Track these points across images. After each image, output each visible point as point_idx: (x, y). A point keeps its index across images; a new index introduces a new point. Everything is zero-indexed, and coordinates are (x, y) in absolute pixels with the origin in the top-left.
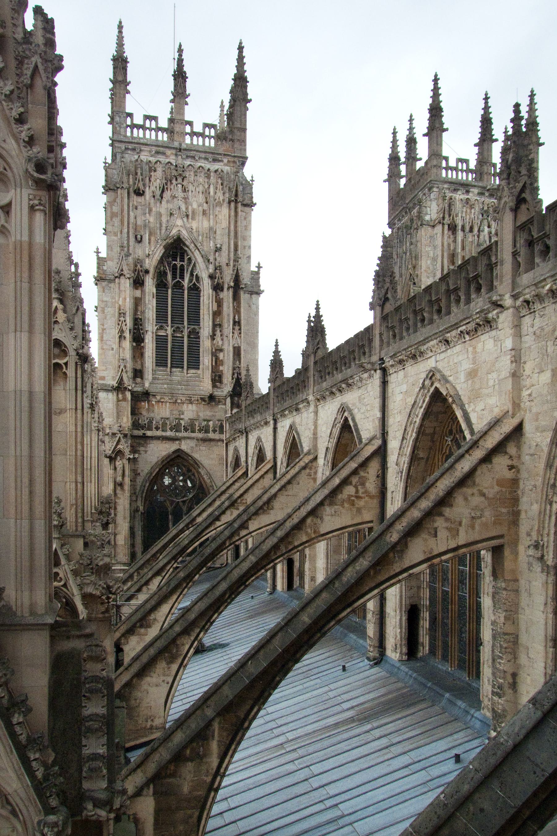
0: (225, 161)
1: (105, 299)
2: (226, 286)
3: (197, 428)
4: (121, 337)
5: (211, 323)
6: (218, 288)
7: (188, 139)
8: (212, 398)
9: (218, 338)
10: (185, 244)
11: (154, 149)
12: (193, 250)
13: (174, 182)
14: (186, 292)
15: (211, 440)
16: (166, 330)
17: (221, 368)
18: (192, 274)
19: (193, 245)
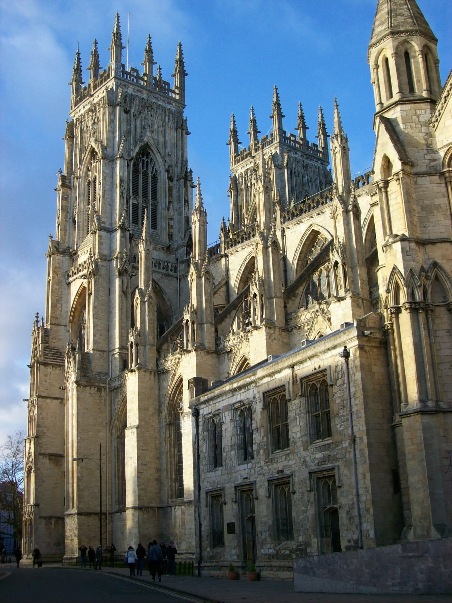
0: (174, 104)
1: (107, 172)
2: (175, 179)
3: (162, 266)
4: (121, 196)
5: (167, 200)
6: (171, 179)
8: (168, 248)
9: (171, 211)
10: (150, 149)
11: (136, 88)
12: (155, 153)
13: (146, 109)
15: (170, 276)
16: (138, 200)
17: (172, 230)
18: (153, 169)
19: (156, 150)
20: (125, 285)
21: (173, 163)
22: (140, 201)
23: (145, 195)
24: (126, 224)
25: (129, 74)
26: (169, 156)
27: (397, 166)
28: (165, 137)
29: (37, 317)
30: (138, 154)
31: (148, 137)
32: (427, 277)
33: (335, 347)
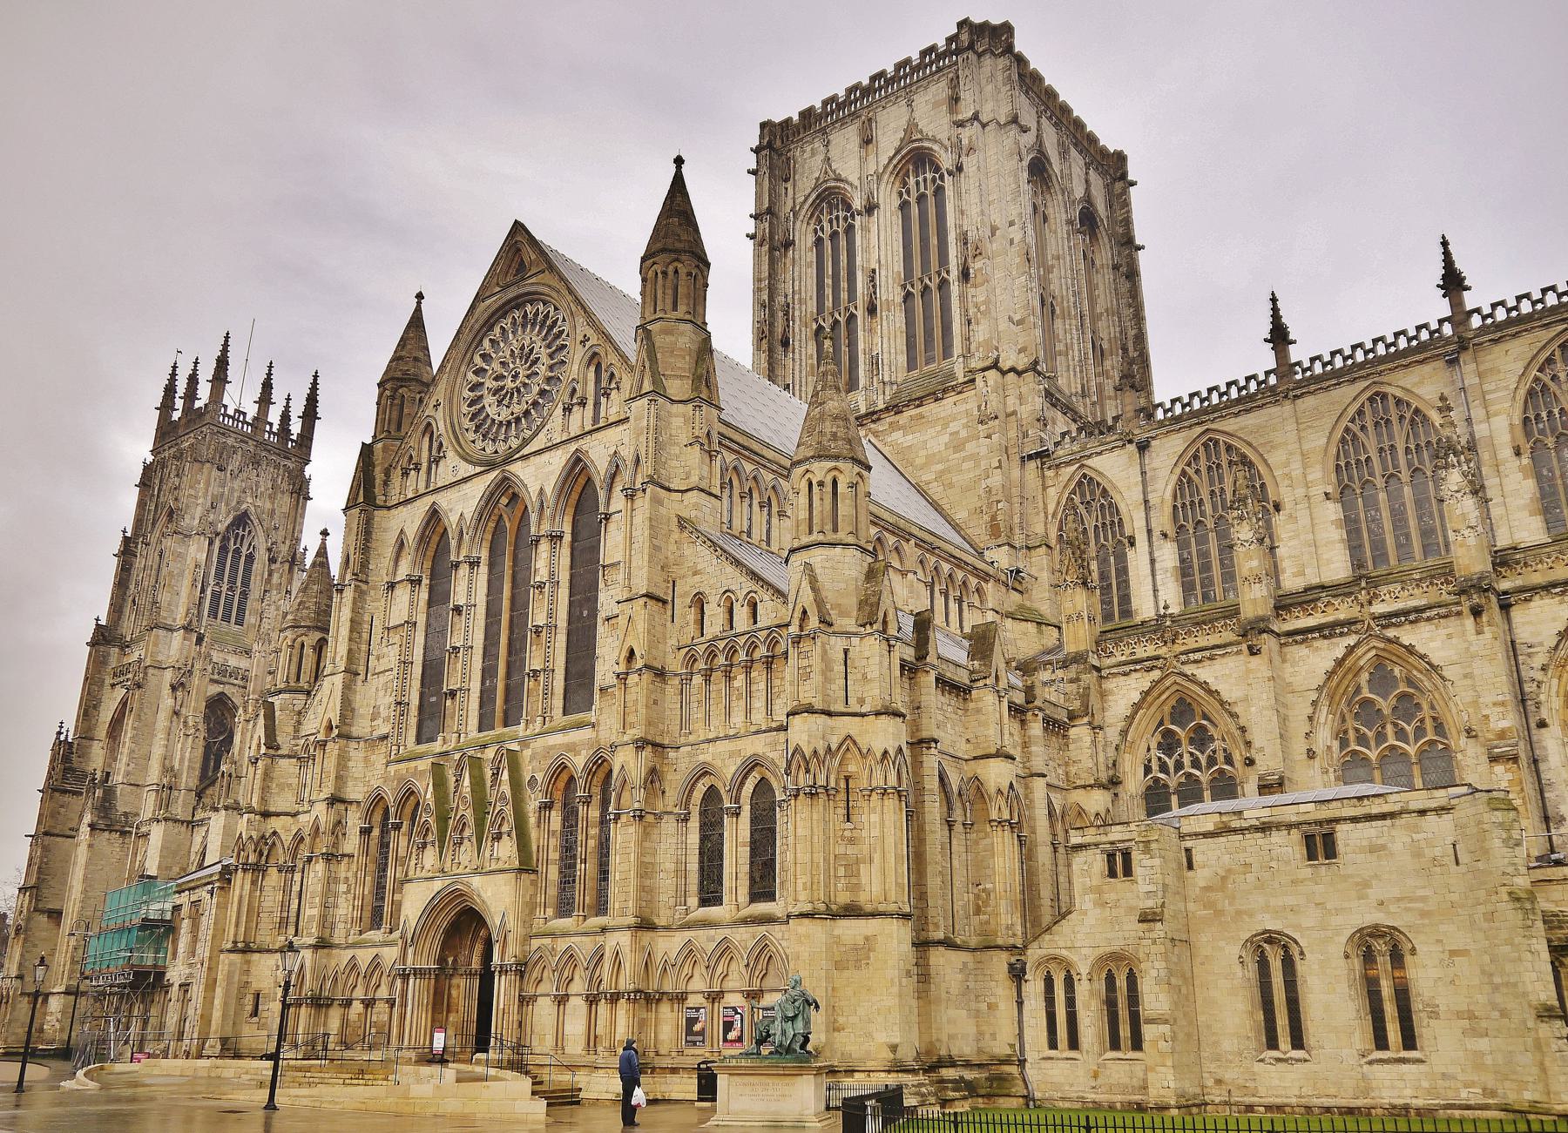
4: (194, 585)
6: (272, 560)
7: (267, 436)
14: (243, 558)
20: (179, 703)
21: (280, 539)
22: (225, 587)
23: (232, 581)
24: (195, 623)
25: (233, 418)
26: (276, 529)
27: (263, 749)
28: (273, 503)
29: (61, 727)
30: (232, 524)
31: (248, 503)
32: (266, 844)
33: (208, 883)
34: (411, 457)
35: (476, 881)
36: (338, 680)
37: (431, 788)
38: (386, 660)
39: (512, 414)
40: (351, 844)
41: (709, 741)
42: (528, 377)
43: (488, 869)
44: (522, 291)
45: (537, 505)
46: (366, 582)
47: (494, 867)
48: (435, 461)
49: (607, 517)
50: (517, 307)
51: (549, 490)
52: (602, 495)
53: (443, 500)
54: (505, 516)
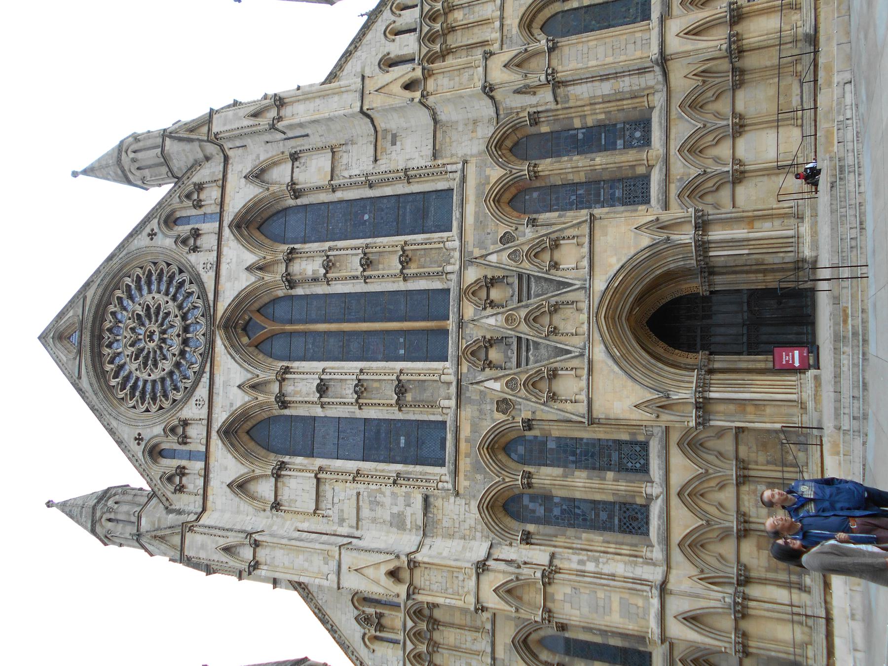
34: (170, 479)
35: (600, 285)
36: (348, 558)
37: (491, 384)
38: (345, 507)
39: (178, 335)
40: (539, 555)
41: (502, 25)
42: (157, 321)
43: (587, 270)
44: (89, 325)
45: (260, 274)
46: (263, 531)
47: (585, 263)
48: (184, 440)
49: (293, 183)
50: (101, 338)
51: (250, 258)
52: (274, 188)
53: (221, 417)
54: (260, 334)
